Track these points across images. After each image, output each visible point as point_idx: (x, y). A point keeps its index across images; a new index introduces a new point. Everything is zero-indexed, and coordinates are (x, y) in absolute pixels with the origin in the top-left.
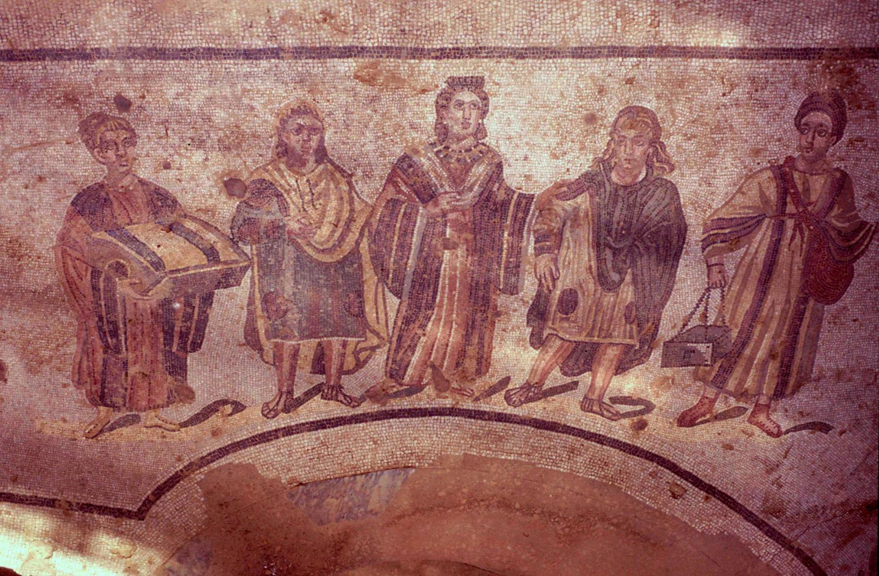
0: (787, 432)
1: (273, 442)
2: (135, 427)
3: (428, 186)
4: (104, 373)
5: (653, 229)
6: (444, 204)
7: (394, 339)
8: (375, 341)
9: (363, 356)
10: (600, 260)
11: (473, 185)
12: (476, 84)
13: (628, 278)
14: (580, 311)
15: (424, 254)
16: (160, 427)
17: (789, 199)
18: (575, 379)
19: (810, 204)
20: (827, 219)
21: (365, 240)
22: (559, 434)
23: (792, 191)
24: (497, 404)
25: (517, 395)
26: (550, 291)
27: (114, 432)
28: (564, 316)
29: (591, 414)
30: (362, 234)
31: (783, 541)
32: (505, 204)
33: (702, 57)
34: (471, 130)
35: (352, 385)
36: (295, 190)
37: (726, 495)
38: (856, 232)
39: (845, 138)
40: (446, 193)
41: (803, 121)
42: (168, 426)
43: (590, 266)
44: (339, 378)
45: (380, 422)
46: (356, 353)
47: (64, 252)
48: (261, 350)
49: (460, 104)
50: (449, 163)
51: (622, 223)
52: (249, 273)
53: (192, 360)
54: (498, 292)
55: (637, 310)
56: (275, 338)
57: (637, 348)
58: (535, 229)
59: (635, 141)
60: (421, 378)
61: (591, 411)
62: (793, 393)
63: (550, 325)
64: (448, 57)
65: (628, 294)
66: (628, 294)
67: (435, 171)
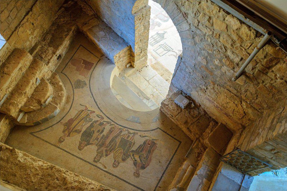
3: (106, 152)
12: (94, 161)
24: (112, 123)
35: (127, 132)
65: (92, 129)
66: (92, 129)
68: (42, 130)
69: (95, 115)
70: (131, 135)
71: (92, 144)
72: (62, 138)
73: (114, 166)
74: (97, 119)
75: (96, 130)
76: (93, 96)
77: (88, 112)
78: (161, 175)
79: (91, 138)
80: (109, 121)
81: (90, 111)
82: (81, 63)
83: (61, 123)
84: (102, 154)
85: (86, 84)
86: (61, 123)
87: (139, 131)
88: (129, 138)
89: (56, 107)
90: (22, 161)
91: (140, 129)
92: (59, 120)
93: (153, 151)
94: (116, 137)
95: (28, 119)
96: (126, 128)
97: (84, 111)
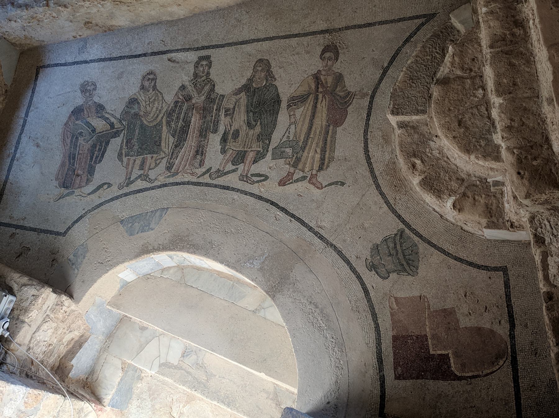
0: (326, 186)
1: (120, 199)
2: (71, 196)
4: (66, 174)
5: (268, 104)
6: (193, 101)
7: (170, 154)
8: (164, 156)
9: (158, 162)
10: (248, 116)
11: (205, 93)
12: (208, 58)
13: (259, 123)
14: (240, 138)
15: (185, 120)
16: (81, 196)
17: (319, 86)
18: (237, 167)
19: (328, 87)
20: (335, 92)
21: (165, 116)
22: (230, 191)
23: (321, 83)
24: (206, 179)
25: (215, 174)
26: (229, 131)
27: (64, 198)
28: (234, 140)
29: (243, 182)
30: (164, 115)
31: (327, 242)
32: (214, 100)
33: (285, 39)
34: (205, 74)
35: (152, 174)
36: (144, 101)
37: (300, 218)
38: (347, 96)
39: (339, 61)
40: (195, 97)
43: (245, 120)
44: (148, 171)
45: (160, 189)
46: (156, 160)
47: (65, 128)
48: (122, 161)
49: (202, 65)
50: (197, 86)
51: (257, 102)
52: (123, 131)
54: (210, 133)
55: (262, 136)
56: (128, 156)
57: (262, 152)
58: (226, 106)
61: (243, 181)
63: (228, 144)
64: (199, 50)
65: (258, 129)
66: (258, 129)
67: (192, 90)
68: (407, 41)
69: (275, 176)
70: (137, 172)
71: (238, 92)
72: (330, 59)
73: (151, 77)
74: (262, 167)
75: (247, 134)
76: (316, 234)
77: (301, 174)
78: (29, 119)
79: (247, 106)
80: (220, 181)
81: (297, 181)
82: (456, 355)
83: (366, 95)
84: (195, 86)
85: (372, 267)
86: (364, 95)
87: (117, 198)
88: (138, 162)
89: (395, 112)
91: (117, 203)
92: (377, 99)
93: (63, 165)
94: (178, 145)
95: (452, 27)
96: (160, 183)
97: (316, 166)
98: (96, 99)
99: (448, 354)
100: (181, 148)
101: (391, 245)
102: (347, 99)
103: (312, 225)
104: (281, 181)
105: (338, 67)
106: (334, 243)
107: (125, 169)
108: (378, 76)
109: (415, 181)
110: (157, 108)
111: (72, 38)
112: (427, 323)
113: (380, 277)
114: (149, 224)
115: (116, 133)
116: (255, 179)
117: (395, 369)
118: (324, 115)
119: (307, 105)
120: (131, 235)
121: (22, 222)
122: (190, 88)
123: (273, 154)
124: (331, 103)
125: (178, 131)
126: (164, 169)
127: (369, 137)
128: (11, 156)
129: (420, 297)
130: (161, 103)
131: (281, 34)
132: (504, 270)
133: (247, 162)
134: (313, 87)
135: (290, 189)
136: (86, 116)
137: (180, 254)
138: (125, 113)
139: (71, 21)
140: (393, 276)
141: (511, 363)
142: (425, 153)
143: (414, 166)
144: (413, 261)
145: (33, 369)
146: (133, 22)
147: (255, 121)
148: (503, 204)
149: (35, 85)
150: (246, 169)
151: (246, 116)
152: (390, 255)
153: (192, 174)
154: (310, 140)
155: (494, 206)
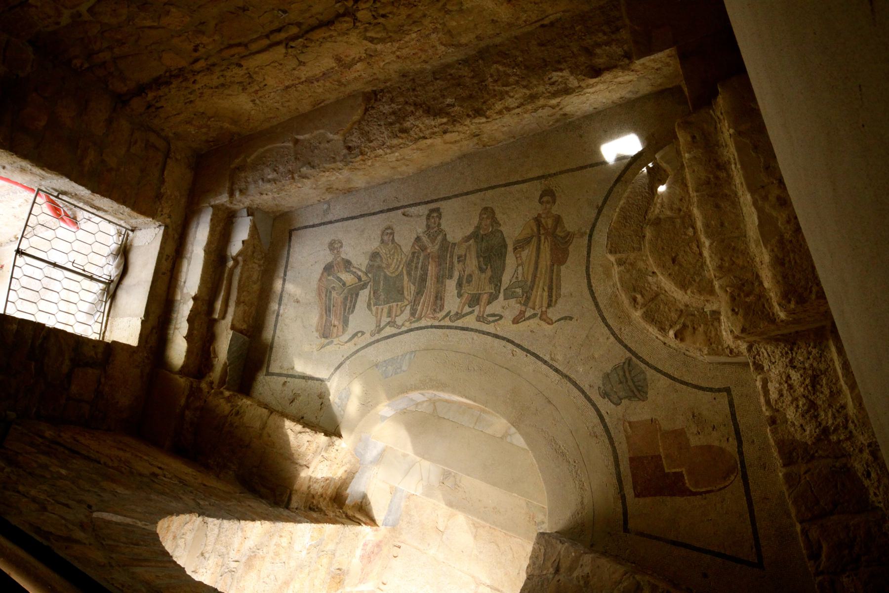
6: (429, 251)
10: (479, 262)
12: (437, 210)
13: (489, 267)
14: (473, 282)
17: (541, 228)
18: (473, 309)
24: (447, 322)
30: (404, 265)
34: (437, 225)
35: (399, 321)
38: (567, 236)
39: (556, 204)
41: (542, 200)
42: (342, 344)
46: (401, 308)
49: (433, 217)
52: (370, 284)
53: (351, 317)
59: (487, 218)
60: (421, 314)
61: (480, 321)
62: (555, 305)
66: (489, 273)
69: (509, 315)
70: (385, 320)
71: (467, 239)
72: (548, 202)
73: (389, 231)
74: (495, 307)
75: (480, 279)
76: (551, 366)
77: (532, 312)
80: (459, 323)
81: (529, 318)
83: (585, 233)
84: (429, 236)
85: (605, 395)
88: (386, 310)
90: (555, 74)
92: (596, 236)
94: (419, 293)
97: (545, 304)
98: (343, 256)
99: (682, 472)
100: (422, 295)
101: (621, 373)
102: (568, 238)
103: (547, 358)
104: (514, 319)
105: (555, 210)
106: (568, 374)
107: (375, 318)
108: (594, 215)
109: (637, 315)
110: (397, 260)
111: (317, 202)
112: (660, 445)
113: (614, 403)
114: (401, 367)
115: (363, 285)
116: (491, 319)
117: (635, 488)
118: (548, 256)
119: (531, 247)
120: (386, 377)
121: (291, 371)
122: (424, 238)
123: (505, 295)
124: (553, 243)
125: (417, 279)
126: (409, 315)
127: (591, 273)
128: (276, 312)
129: (652, 419)
130: (400, 254)
131: (501, 183)
132: (728, 390)
133: (482, 304)
134: (535, 230)
135: (523, 326)
136: (336, 271)
137: (431, 391)
138: (370, 268)
139: (315, 189)
140: (625, 402)
141: (742, 477)
142: (644, 288)
143: (635, 300)
144: (642, 387)
145: (314, 502)
146: (369, 183)
147: (485, 265)
148: (721, 331)
149: (290, 246)
150: (482, 310)
151: (477, 262)
152: (621, 383)
153: (434, 318)
154: (537, 279)
155: (713, 333)
